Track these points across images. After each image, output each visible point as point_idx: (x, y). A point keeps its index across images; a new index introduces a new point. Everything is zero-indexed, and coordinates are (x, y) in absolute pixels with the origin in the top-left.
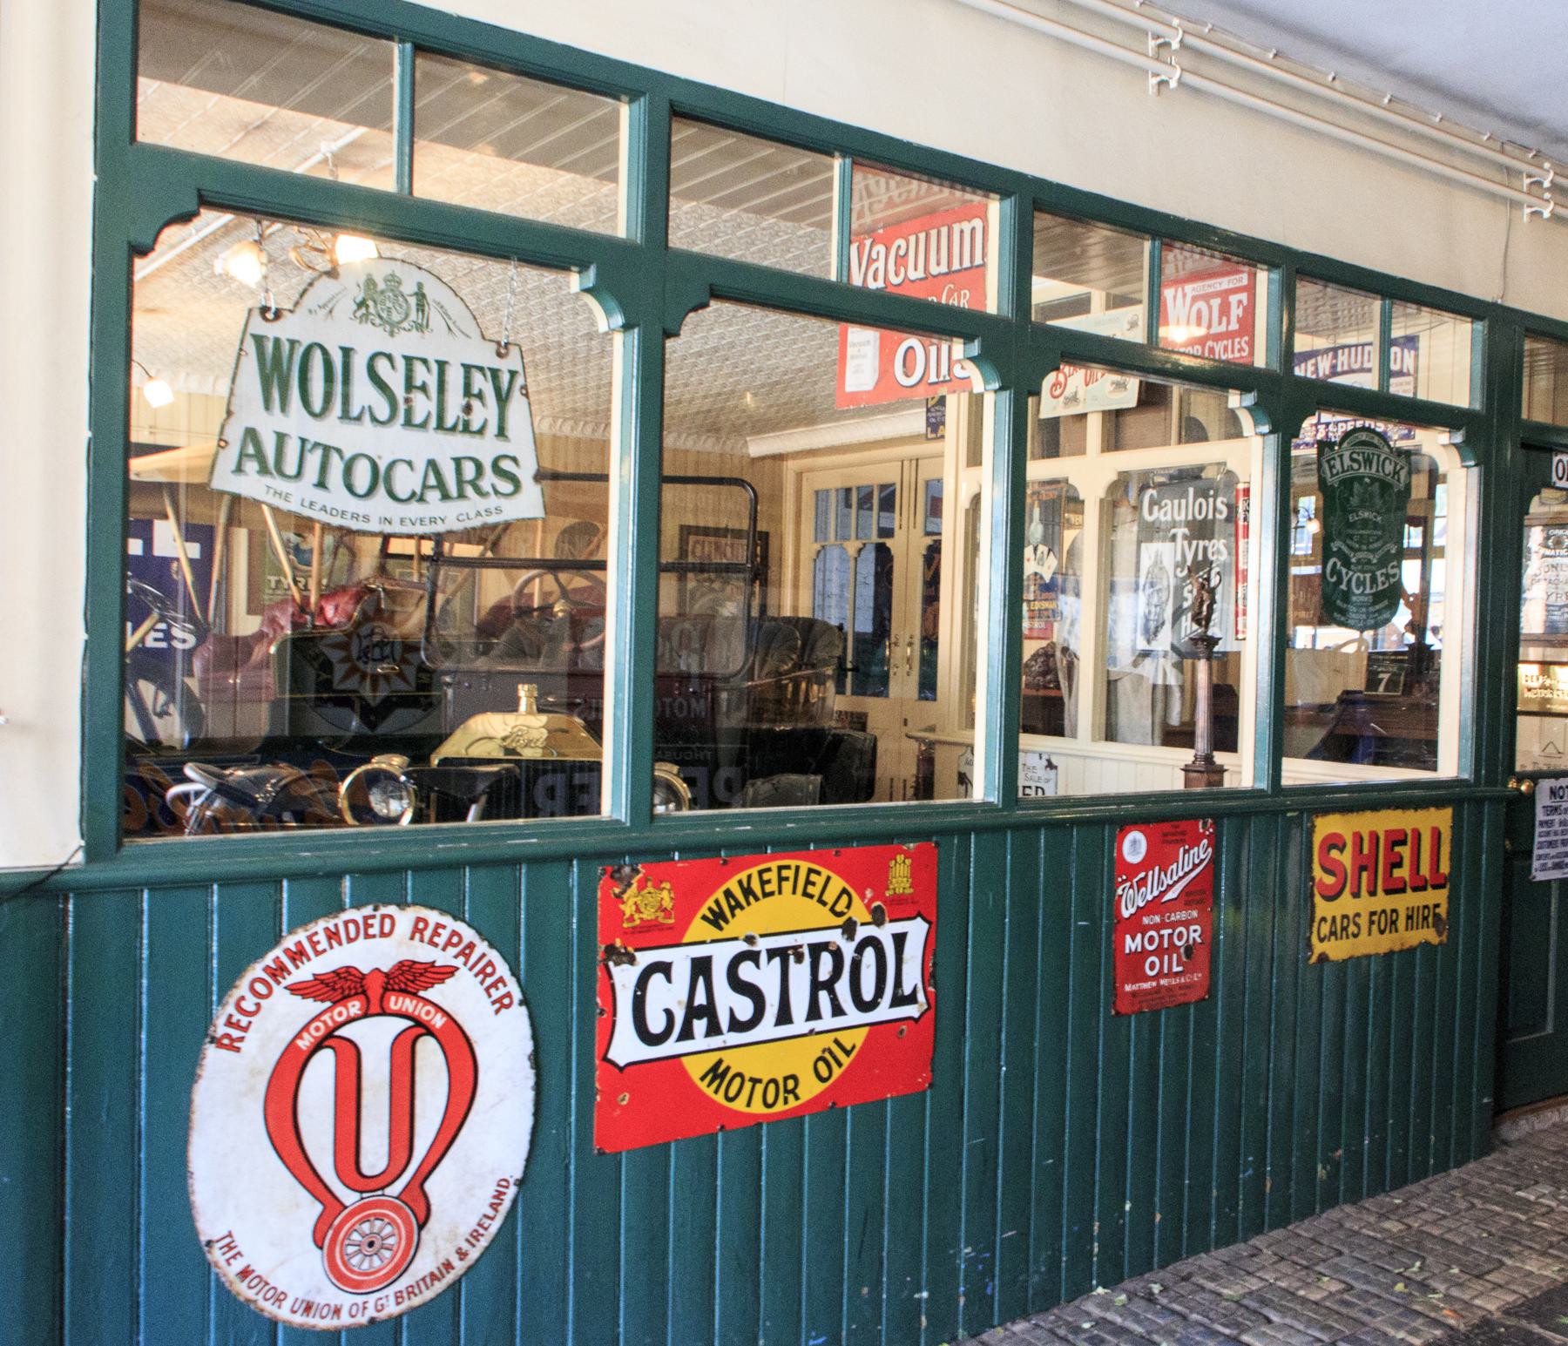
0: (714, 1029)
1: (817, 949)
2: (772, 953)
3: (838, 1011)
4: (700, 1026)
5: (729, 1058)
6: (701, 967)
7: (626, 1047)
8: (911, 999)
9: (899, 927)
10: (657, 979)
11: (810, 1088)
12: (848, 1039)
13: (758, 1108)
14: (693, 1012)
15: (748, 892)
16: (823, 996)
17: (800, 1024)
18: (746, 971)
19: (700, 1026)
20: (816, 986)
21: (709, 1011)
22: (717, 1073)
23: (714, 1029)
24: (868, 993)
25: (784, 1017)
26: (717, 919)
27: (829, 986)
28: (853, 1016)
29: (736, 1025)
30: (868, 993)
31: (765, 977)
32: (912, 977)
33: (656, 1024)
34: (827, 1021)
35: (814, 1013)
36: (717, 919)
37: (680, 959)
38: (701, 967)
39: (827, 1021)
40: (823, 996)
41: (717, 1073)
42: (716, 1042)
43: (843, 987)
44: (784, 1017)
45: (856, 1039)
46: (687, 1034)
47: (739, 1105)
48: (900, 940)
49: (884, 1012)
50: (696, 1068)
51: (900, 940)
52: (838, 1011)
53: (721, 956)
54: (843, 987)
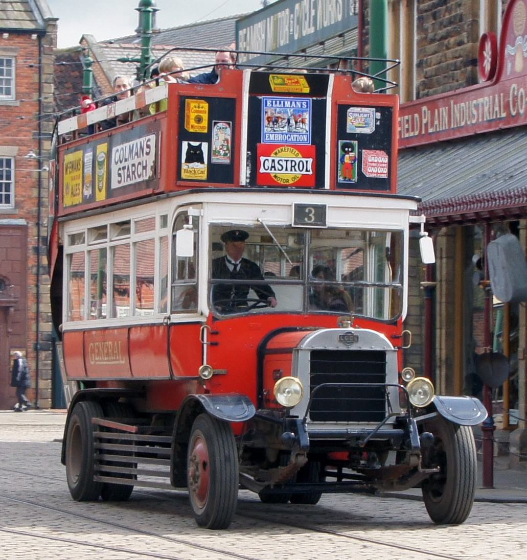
0: (275, 170)
1: (292, 161)
2: (285, 160)
3: (295, 170)
4: (273, 169)
5: (277, 175)
6: (273, 161)
7: (262, 170)
8: (309, 171)
9: (307, 159)
10: (266, 161)
11: (291, 182)
12: (298, 176)
13: (282, 183)
14: (272, 167)
15: (282, 150)
16: (293, 168)
17: (289, 171)
18: (280, 162)
19: (273, 169)
20: (292, 166)
21: (274, 167)
22: (275, 176)
23: (275, 170)
24: (301, 169)
25: (286, 170)
26: (276, 154)
27: (294, 166)
28: (298, 172)
29: (279, 170)
30: (301, 169)
31: (284, 164)
32: (310, 168)
33: (267, 168)
34: (293, 172)
35: (291, 170)
36: (276, 154)
37: (270, 159)
38: (273, 161)
39: (293, 172)
40: (293, 168)
41: (275, 176)
42: (275, 172)
43: (297, 167)
44: (286, 170)
45: (300, 176)
46: (271, 170)
47: (279, 182)
48: (307, 162)
49: (304, 172)
50: (272, 175)
51: (307, 162)
52: (295, 170)
53: (276, 160)
54: (297, 167)
